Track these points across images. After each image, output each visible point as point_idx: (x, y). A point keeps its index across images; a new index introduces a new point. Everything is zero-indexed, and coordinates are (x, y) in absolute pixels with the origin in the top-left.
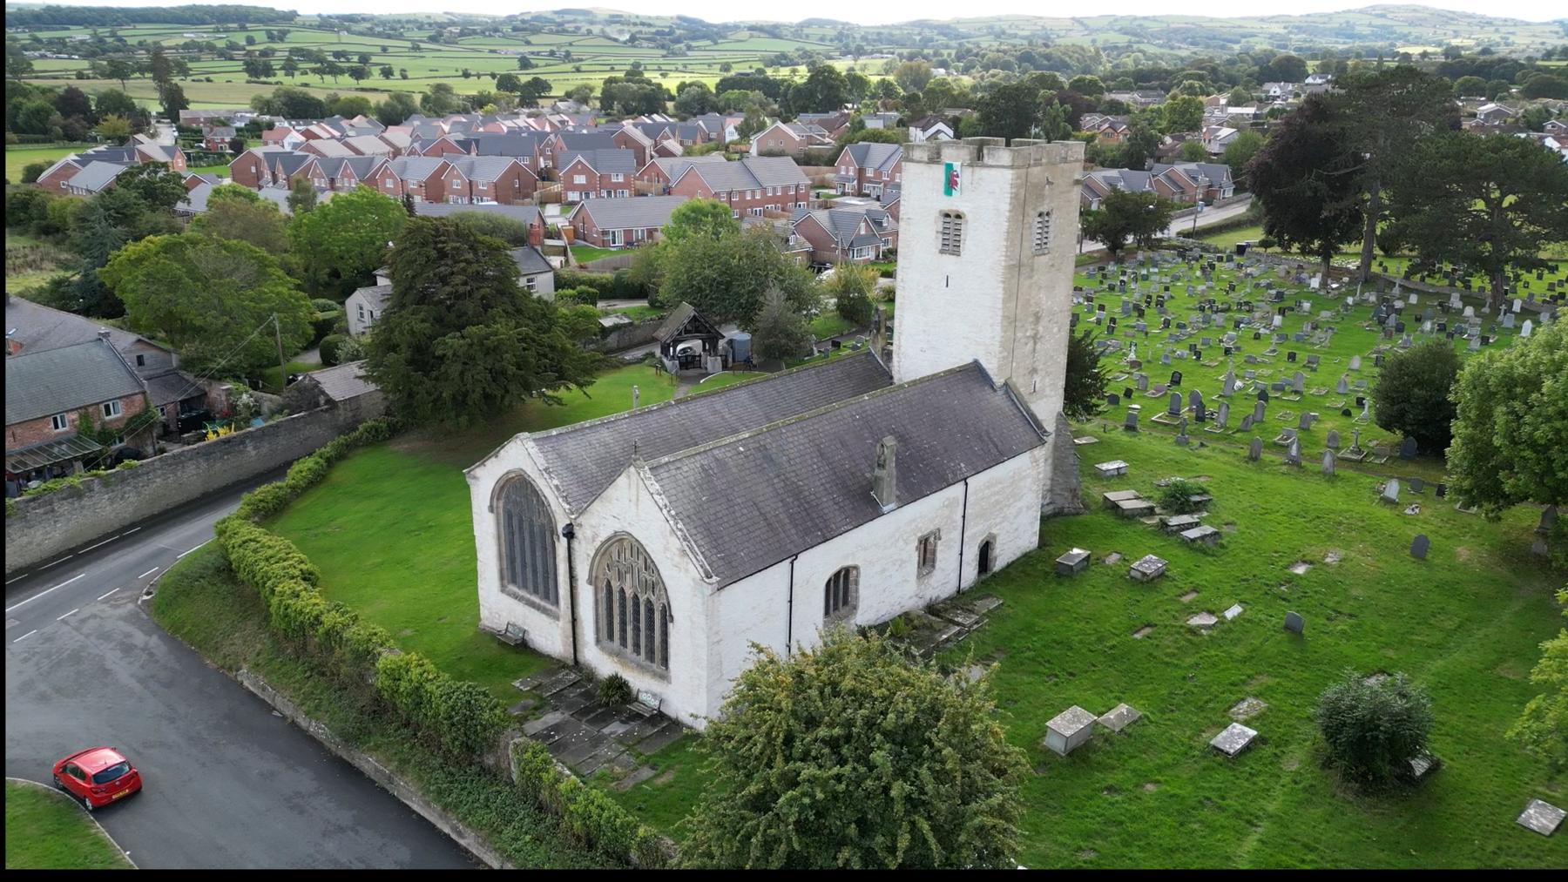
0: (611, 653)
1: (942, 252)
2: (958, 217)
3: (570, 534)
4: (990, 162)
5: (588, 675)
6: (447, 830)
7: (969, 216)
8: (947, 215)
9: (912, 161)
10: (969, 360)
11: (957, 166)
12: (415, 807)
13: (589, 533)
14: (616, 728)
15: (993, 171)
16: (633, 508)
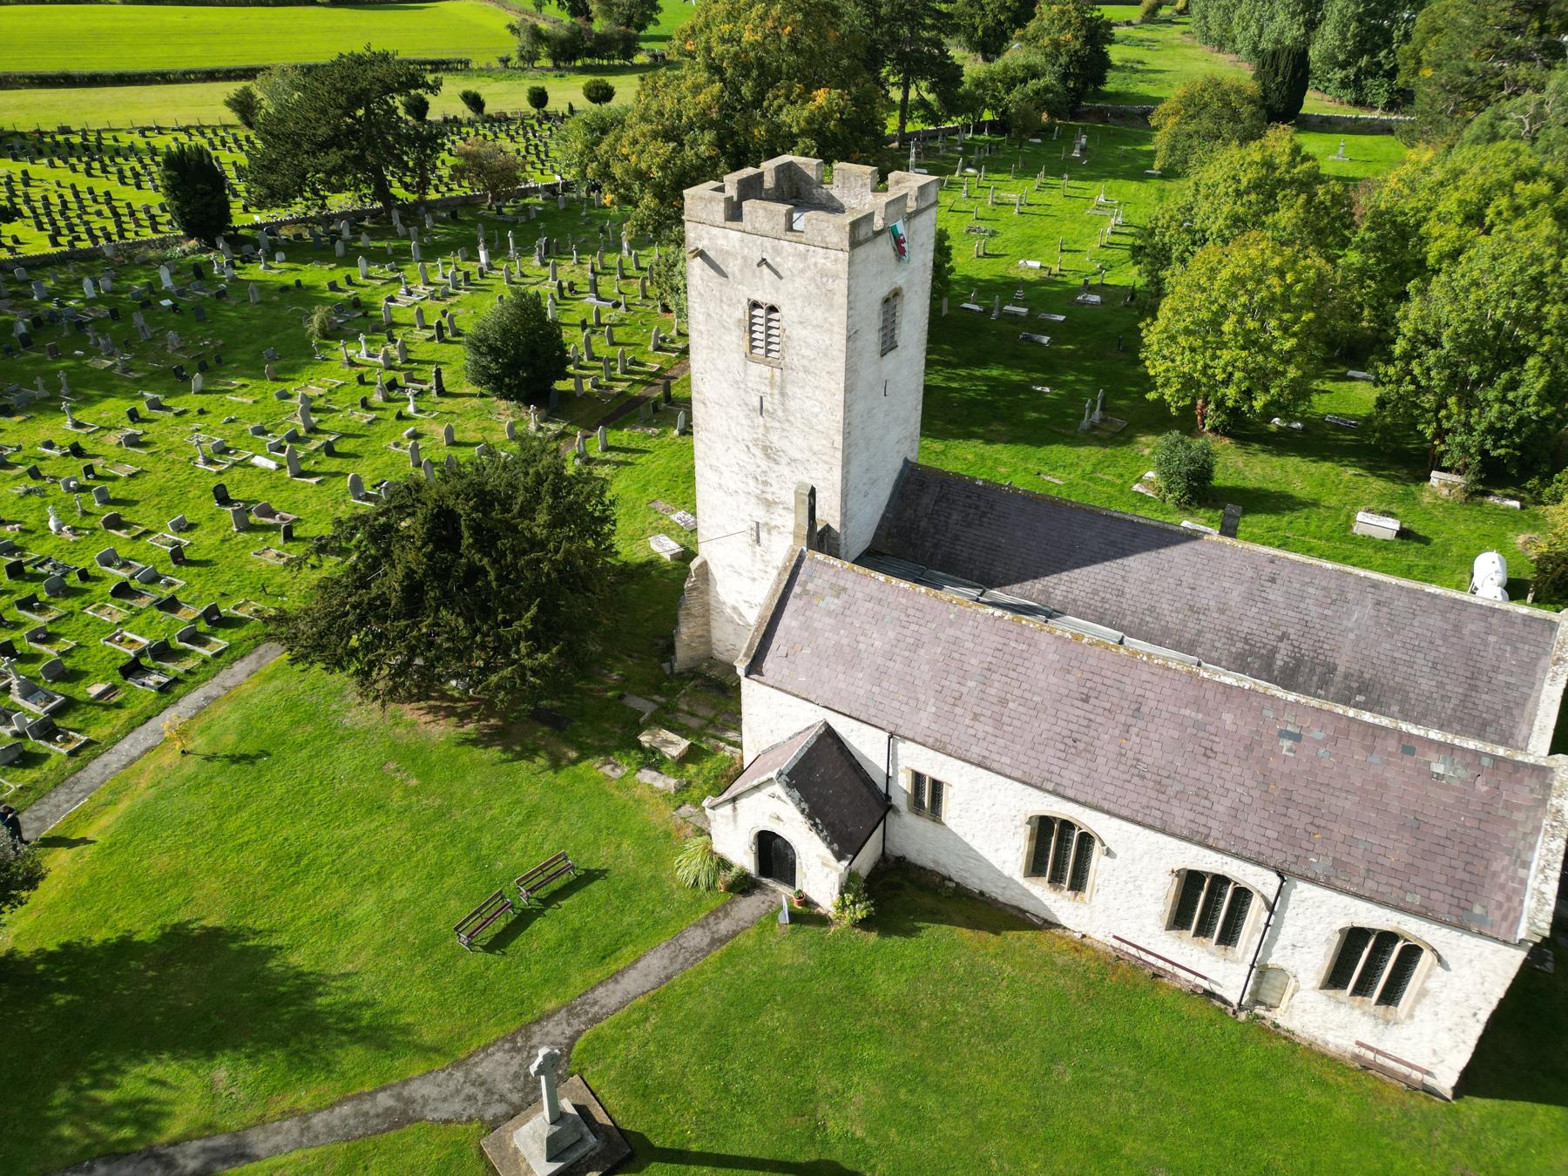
10: (899, 465)
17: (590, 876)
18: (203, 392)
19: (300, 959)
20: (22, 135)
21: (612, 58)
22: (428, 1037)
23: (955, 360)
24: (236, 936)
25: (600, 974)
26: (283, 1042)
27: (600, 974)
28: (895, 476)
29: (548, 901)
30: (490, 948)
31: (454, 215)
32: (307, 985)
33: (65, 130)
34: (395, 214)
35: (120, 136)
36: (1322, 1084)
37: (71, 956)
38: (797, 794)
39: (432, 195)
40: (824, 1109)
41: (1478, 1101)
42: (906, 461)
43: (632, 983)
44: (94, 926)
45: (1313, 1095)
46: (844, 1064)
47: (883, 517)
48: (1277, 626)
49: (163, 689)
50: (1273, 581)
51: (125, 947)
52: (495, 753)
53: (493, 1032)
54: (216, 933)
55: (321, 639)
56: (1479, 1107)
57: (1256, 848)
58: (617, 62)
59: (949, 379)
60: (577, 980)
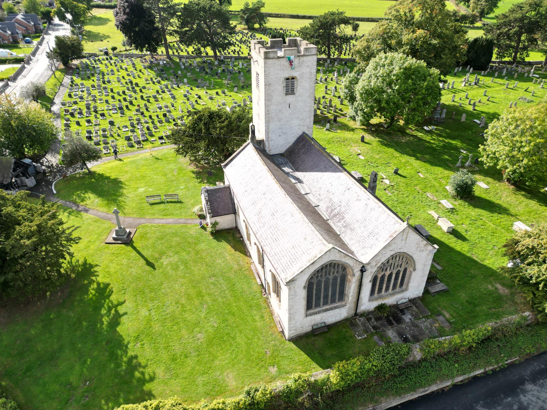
0: (377, 299)
1: (286, 94)
2: (293, 78)
3: (363, 271)
4: (307, 54)
5: (367, 315)
6: (417, 396)
7: (298, 78)
8: (288, 79)
9: (269, 58)
11: (292, 58)
12: (394, 405)
13: (374, 264)
14: (407, 318)
15: (308, 58)
16: (404, 242)
17: (180, 202)
18: (236, 92)
19: (125, 191)
20: (271, 29)
21: (466, 23)
22: (126, 211)
23: (444, 135)
24: (122, 184)
25: (161, 217)
26: (108, 200)
27: (161, 217)
28: (298, 136)
29: (168, 202)
30: (150, 204)
31: (346, 63)
32: (122, 195)
33: (281, 29)
34: (329, 61)
35: (291, 32)
36: (262, 317)
37: (101, 176)
38: (207, 194)
39: (342, 56)
40: (164, 257)
41: (293, 344)
42: (304, 133)
43: (162, 221)
44: (109, 173)
45: (257, 318)
46: (177, 253)
47: (290, 147)
48: (341, 202)
49: (162, 143)
50: (349, 189)
51: (108, 178)
52: (194, 175)
53: (135, 216)
54: (120, 182)
55: (175, 137)
56: (292, 346)
57: (262, 239)
58: (467, 25)
59: (434, 139)
60: (156, 216)
